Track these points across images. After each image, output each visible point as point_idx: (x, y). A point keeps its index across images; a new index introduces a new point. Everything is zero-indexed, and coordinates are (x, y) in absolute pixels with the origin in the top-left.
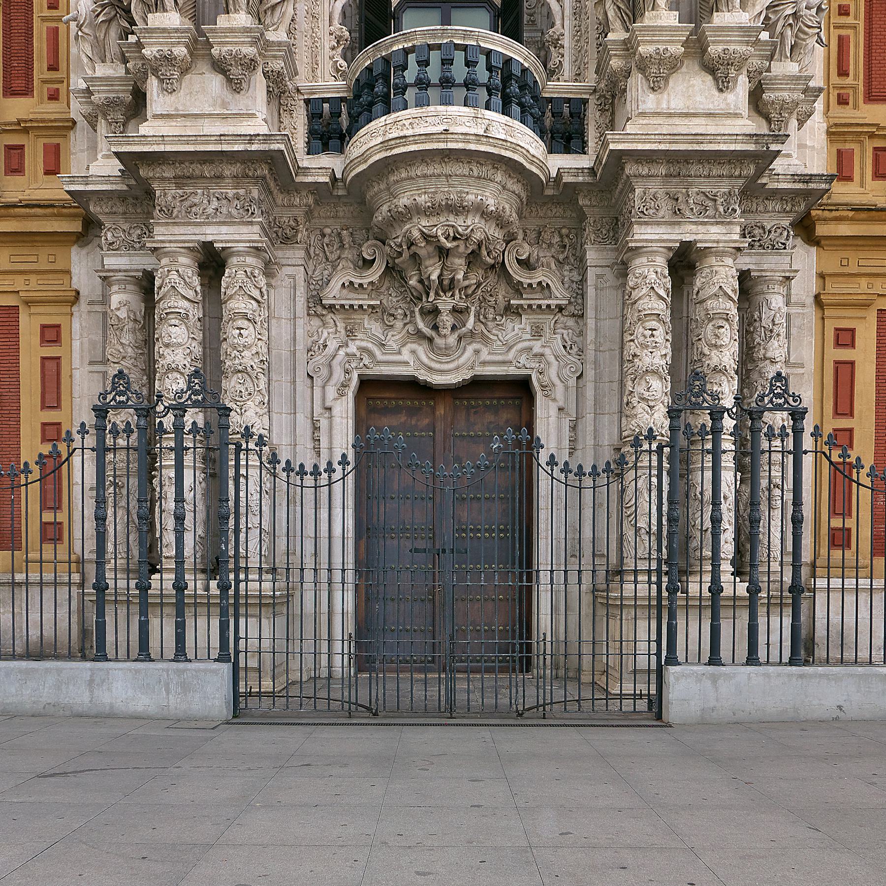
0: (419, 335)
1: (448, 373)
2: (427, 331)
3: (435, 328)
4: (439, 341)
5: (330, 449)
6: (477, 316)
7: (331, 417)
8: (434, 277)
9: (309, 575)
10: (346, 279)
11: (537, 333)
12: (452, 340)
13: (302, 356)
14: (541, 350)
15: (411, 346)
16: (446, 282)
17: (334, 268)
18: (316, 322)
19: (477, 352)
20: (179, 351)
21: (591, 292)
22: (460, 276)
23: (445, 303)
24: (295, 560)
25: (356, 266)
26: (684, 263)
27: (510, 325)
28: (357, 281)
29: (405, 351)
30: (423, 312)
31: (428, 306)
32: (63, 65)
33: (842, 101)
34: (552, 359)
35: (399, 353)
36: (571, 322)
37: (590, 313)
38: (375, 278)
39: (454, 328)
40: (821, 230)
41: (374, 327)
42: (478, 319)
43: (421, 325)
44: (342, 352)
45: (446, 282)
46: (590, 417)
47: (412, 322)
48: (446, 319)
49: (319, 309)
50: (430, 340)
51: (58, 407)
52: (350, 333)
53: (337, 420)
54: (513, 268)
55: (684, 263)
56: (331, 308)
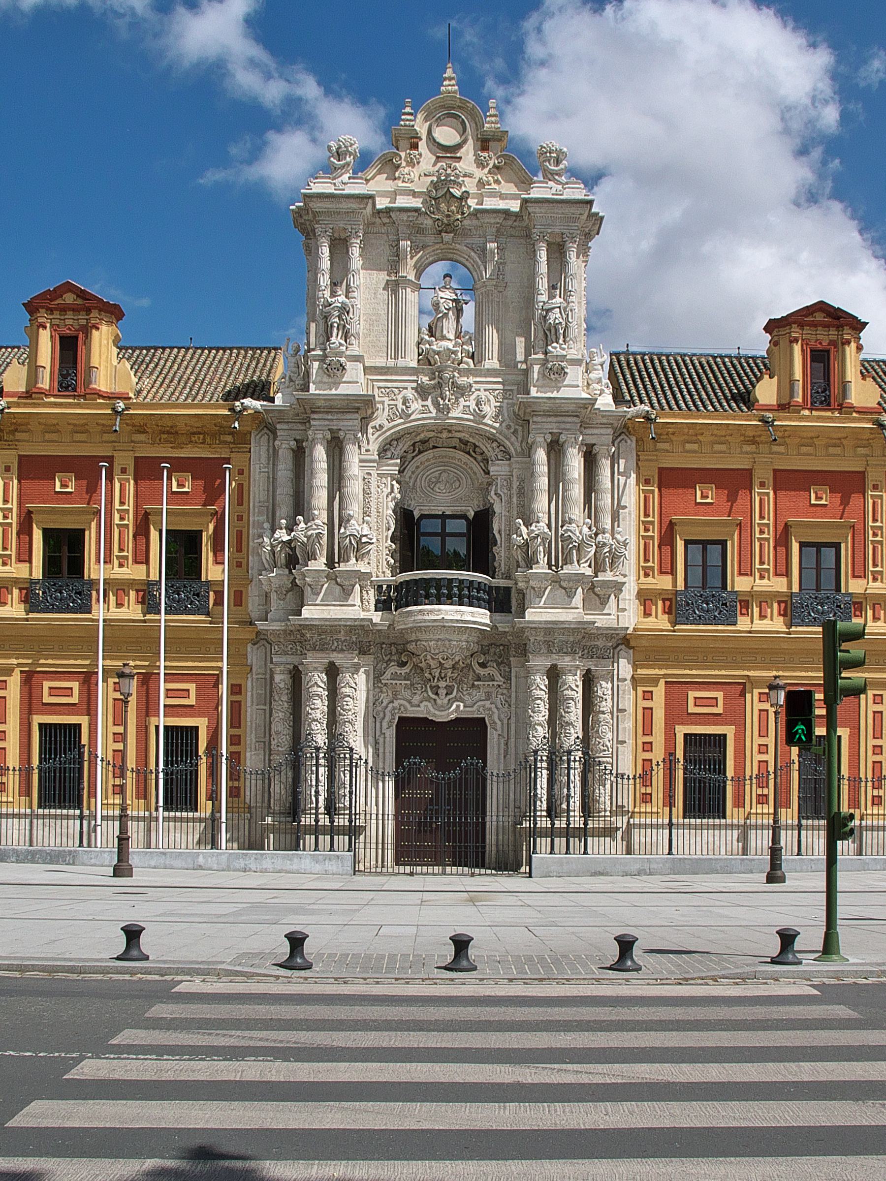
0: (428, 699)
1: (442, 717)
2: (434, 696)
3: (437, 694)
4: (439, 702)
5: (384, 753)
6: (458, 688)
7: (385, 738)
8: (437, 675)
9: (374, 817)
10: (393, 671)
11: (488, 697)
12: (446, 701)
13: (371, 709)
14: (490, 706)
15: (425, 703)
16: (443, 675)
17: (388, 665)
18: (377, 690)
19: (458, 706)
20: (318, 711)
21: (513, 679)
22: (449, 674)
23: (442, 684)
24: (368, 809)
25: (398, 663)
26: (554, 675)
27: (474, 693)
28: (398, 672)
29: (422, 705)
30: (431, 686)
31: (434, 684)
32: (244, 549)
33: (646, 575)
34: (495, 710)
35: (419, 706)
36: (505, 691)
37: (513, 689)
38: (408, 671)
39: (447, 694)
40: (632, 644)
41: (407, 694)
42: (458, 691)
43: (430, 693)
44: (391, 705)
45: (443, 675)
46: (513, 740)
47: (426, 691)
48: (442, 692)
49: (380, 685)
50: (435, 700)
51: (239, 727)
52: (395, 697)
53: (388, 739)
54: (476, 667)
55: (554, 675)
56: (386, 685)
